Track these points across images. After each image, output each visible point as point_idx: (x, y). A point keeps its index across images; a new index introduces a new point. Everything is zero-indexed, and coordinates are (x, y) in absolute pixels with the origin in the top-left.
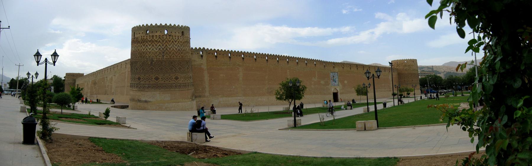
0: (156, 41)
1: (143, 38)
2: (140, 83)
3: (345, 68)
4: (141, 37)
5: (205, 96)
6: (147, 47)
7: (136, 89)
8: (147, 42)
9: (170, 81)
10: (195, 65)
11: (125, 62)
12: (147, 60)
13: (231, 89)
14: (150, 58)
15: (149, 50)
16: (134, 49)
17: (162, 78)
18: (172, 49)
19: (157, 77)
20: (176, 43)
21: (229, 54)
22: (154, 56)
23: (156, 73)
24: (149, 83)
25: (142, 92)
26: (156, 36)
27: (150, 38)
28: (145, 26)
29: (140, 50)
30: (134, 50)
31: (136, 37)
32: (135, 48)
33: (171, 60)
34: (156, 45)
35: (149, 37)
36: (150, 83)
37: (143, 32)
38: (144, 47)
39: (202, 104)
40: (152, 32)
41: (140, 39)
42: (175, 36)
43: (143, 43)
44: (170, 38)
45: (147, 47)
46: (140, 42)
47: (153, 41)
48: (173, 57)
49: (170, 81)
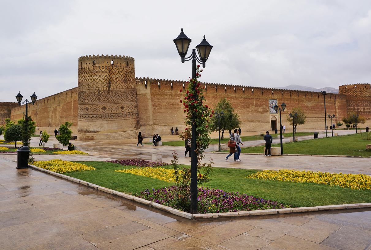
0: (103, 72)
3: (285, 95)
4: (89, 67)
5: (149, 125)
7: (84, 120)
9: (116, 111)
10: (140, 94)
11: (71, 91)
12: (95, 90)
13: (174, 118)
16: (81, 80)
19: (104, 107)
20: (121, 74)
21: (171, 83)
24: (96, 113)
25: (90, 122)
26: (103, 67)
28: (92, 56)
29: (87, 80)
31: (83, 67)
33: (117, 90)
34: (103, 76)
36: (98, 113)
39: (147, 132)
41: (87, 69)
42: (121, 67)
44: (116, 69)
46: (87, 73)
47: (100, 72)
48: (119, 87)
49: (116, 111)
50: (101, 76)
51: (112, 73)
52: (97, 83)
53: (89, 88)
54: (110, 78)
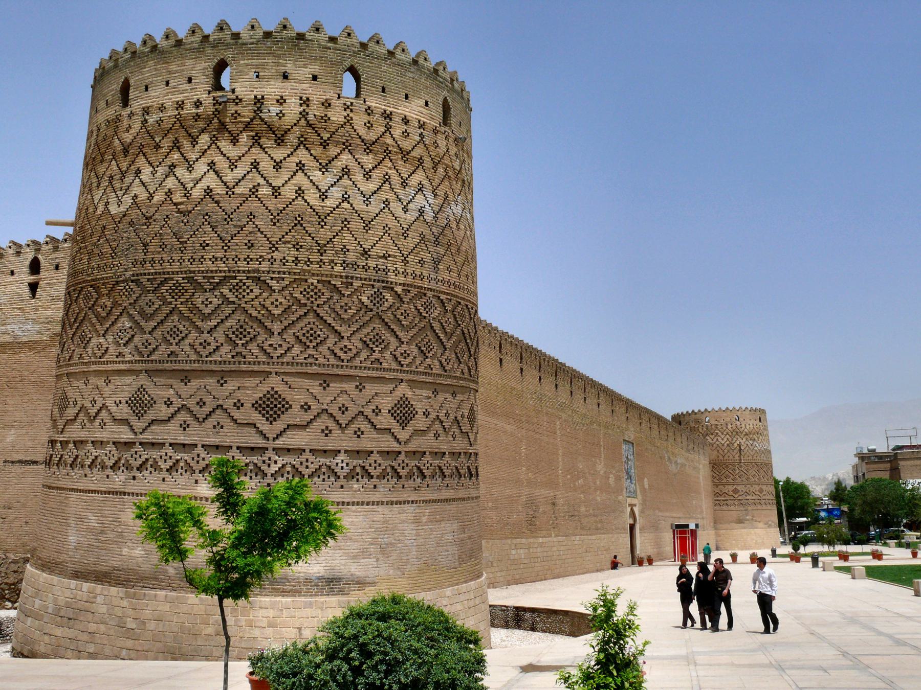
0: (405, 154)
1: (315, 111)
2: (280, 442)
4: (306, 102)
6: (345, 181)
8: (347, 146)
12: (351, 272)
14: (372, 263)
15: (358, 202)
16: (211, 180)
19: (404, 403)
22: (393, 251)
23: (400, 375)
24: (354, 444)
26: (406, 121)
29: (288, 192)
30: (219, 190)
32: (230, 177)
33: (461, 294)
34: (404, 184)
35: (366, 118)
36: (366, 443)
37: (315, 68)
40: (383, 90)
46: (292, 139)
47: (387, 152)
50: (396, 180)
51: (446, 181)
52: (367, 226)
53: (297, 247)
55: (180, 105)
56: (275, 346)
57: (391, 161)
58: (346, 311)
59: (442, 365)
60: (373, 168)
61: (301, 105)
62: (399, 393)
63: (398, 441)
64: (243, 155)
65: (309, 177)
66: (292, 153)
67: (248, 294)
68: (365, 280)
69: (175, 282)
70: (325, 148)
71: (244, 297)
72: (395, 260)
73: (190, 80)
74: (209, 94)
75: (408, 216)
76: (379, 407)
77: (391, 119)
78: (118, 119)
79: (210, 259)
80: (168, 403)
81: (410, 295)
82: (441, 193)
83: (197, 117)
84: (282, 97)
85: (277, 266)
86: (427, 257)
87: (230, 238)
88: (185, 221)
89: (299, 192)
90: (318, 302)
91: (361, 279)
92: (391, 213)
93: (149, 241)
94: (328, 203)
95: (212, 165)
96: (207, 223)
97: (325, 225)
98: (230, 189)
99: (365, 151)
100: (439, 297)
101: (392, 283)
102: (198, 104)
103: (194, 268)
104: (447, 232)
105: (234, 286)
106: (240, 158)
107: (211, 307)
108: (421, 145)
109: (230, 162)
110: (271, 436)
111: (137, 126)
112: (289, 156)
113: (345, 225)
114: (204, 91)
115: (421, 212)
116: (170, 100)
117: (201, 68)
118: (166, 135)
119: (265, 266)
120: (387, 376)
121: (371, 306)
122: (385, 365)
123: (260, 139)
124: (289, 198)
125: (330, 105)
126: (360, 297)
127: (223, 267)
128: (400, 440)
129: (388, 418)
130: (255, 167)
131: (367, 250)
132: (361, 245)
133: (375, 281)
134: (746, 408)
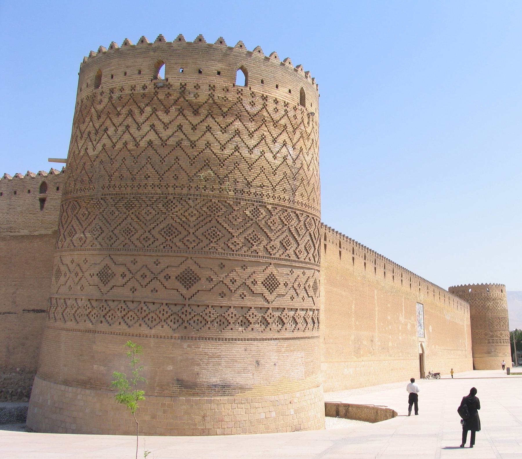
0: (276, 124)
8: (239, 117)
12: (239, 196)
14: (253, 190)
15: (245, 152)
16: (152, 136)
17: (286, 285)
18: (311, 169)
19: (272, 277)
22: (266, 183)
23: (269, 261)
26: (276, 101)
27: (253, 104)
30: (157, 142)
33: (309, 210)
37: (219, 66)
38: (223, 138)
43: (220, 119)
45: (237, 139)
46: (204, 112)
47: (264, 121)
49: (303, 299)
50: (269, 139)
52: (250, 167)
54: (295, 157)
55: (133, 88)
56: (190, 241)
57: (266, 127)
58: (236, 220)
59: (296, 254)
60: (255, 131)
61: (210, 90)
62: (268, 272)
63: (268, 301)
64: (173, 121)
65: (214, 136)
66: (203, 120)
67: (174, 208)
68: (248, 200)
69: (128, 200)
70: (224, 117)
71: (171, 209)
72: (268, 188)
73: (140, 72)
74: (152, 81)
75: (276, 161)
76: (256, 280)
77: (267, 100)
78: (94, 96)
79: (151, 186)
80: (123, 276)
81: (276, 211)
82: (298, 147)
83: (144, 96)
84: (198, 85)
85: (192, 191)
86: (287, 187)
87: (163, 173)
88: (135, 162)
89: (207, 145)
90: (218, 214)
91: (246, 200)
92: (266, 159)
93: (112, 174)
94: (226, 152)
95: (153, 126)
96: (149, 163)
97: (224, 166)
98: (164, 144)
99: (250, 120)
100: (295, 213)
101: (265, 203)
102: (144, 87)
103: (140, 191)
104: (301, 171)
105: (165, 203)
106: (170, 123)
107: (150, 216)
108: (286, 117)
109: (164, 125)
110: (187, 297)
111: (106, 100)
112: (201, 122)
113: (236, 166)
114: (149, 79)
115: (285, 159)
116: (127, 83)
117: (145, 64)
118: (124, 106)
119: (185, 191)
120: (261, 261)
121: (252, 217)
122: (260, 254)
123: (183, 110)
124: (200, 149)
125: (228, 90)
126: (245, 211)
127: (159, 191)
128: (269, 301)
129: (261, 287)
130: (180, 129)
131: (250, 182)
132: (246, 179)
133: (254, 201)
134: (494, 284)
